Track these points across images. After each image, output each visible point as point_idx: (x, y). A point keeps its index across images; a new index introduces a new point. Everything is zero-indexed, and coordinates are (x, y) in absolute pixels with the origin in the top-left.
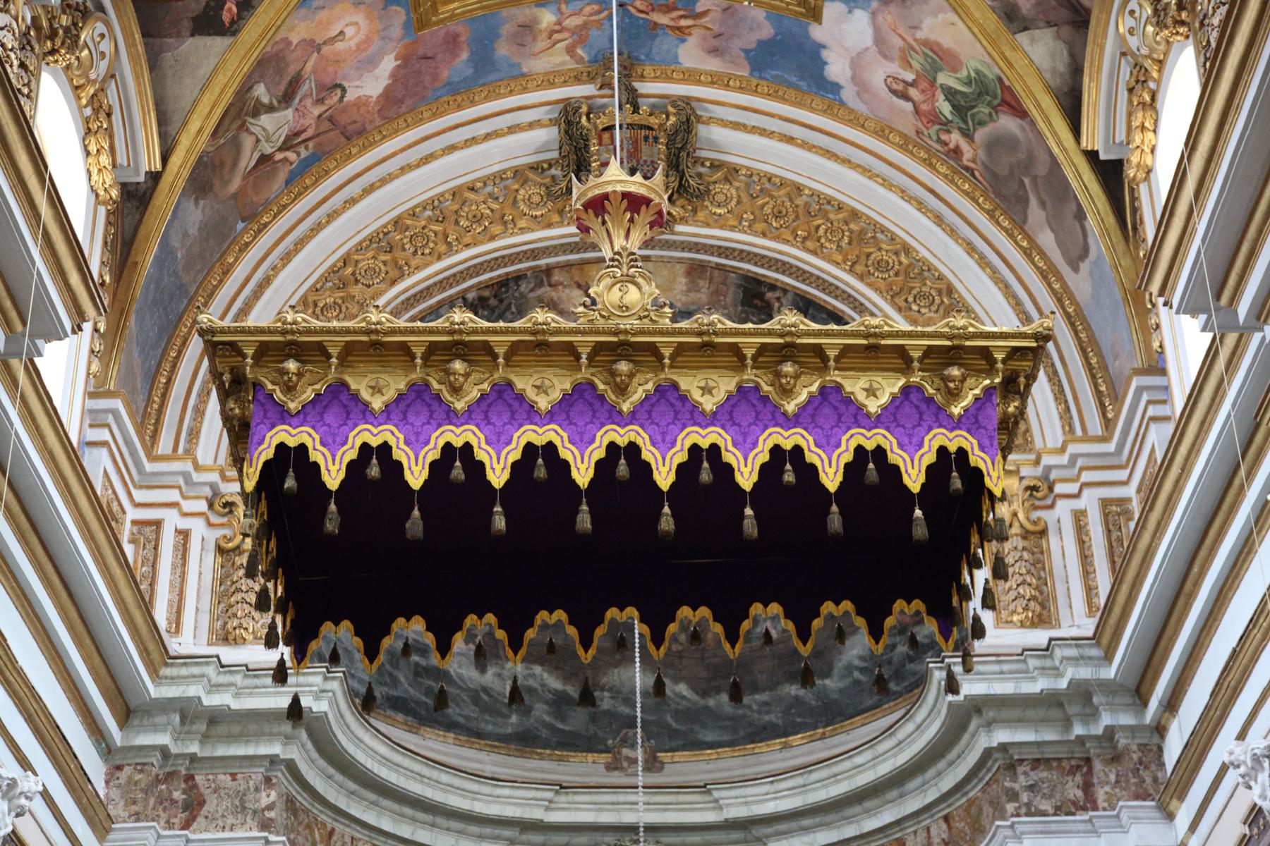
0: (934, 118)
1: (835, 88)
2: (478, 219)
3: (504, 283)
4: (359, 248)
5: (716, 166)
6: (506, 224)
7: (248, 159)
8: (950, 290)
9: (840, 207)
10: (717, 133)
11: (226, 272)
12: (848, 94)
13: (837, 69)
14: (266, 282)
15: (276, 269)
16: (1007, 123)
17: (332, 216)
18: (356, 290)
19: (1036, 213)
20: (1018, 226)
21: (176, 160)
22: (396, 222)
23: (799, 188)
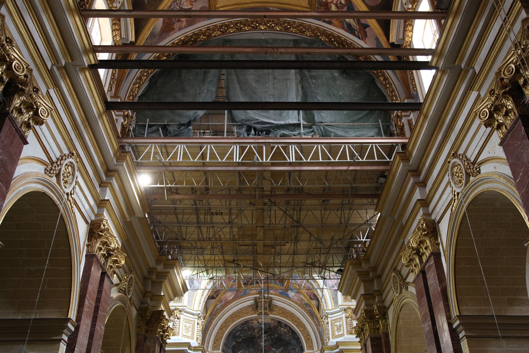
0: (302, 304)
1: (290, 297)
2: (243, 313)
3: (247, 321)
4: (228, 318)
5: (275, 305)
6: (248, 314)
7: (216, 309)
8: (304, 325)
9: (291, 312)
10: (275, 301)
11: (212, 323)
12: (292, 298)
13: (290, 296)
14: (217, 324)
15: (218, 322)
16: (310, 308)
17: (225, 314)
18: (228, 324)
19: (315, 318)
20: (312, 319)
21: (208, 314)
22: (233, 314)
23: (285, 309)
